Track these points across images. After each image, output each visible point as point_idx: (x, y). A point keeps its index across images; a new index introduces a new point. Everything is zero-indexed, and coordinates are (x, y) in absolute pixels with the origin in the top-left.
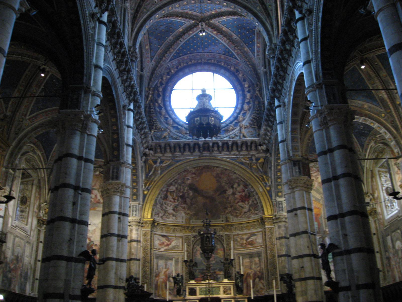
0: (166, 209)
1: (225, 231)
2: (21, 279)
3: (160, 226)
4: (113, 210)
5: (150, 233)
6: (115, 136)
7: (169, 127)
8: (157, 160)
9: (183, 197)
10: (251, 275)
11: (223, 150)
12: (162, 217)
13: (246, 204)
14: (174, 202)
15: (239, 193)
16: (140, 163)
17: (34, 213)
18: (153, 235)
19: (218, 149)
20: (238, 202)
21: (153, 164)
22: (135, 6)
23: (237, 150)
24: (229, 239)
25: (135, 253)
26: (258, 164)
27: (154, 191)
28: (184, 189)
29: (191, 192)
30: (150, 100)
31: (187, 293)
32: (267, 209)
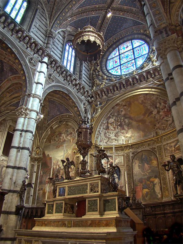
8: (97, 103)
11: (141, 81)
12: (106, 143)
14: (115, 130)
15: (163, 110)
19: (137, 82)
22: (51, 9)
28: (121, 120)
29: (126, 120)
30: (93, 70)
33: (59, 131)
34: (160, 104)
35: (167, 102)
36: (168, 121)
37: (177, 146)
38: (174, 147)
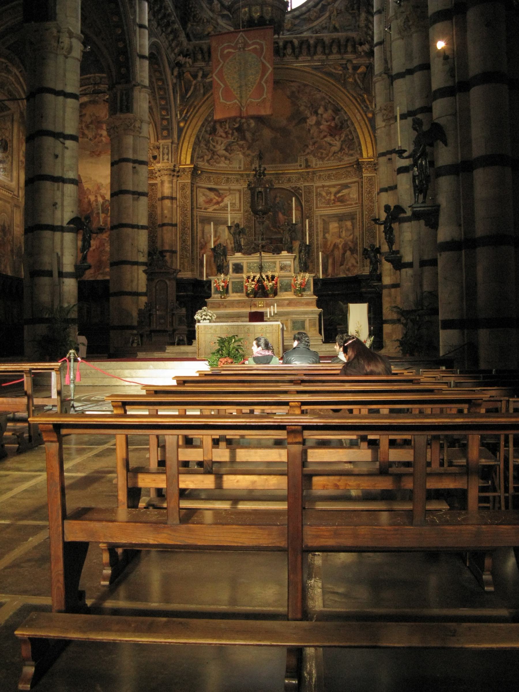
0: (215, 149)
1: (304, 182)
2: (13, 258)
3: (205, 175)
4: (125, 156)
5: (189, 186)
6: (121, 45)
7: (216, 16)
8: (198, 72)
9: (239, 130)
10: (340, 246)
11: (300, 52)
12: (208, 161)
13: (336, 140)
14: (227, 137)
15: (327, 122)
16: (171, 80)
17: (20, 163)
18: (195, 188)
20: (325, 137)
21: (192, 79)
23: (324, 53)
24: (310, 193)
25: (169, 216)
26: (356, 76)
27: (194, 121)
31: (231, 270)
32: (367, 147)
33: (94, 115)
34: (326, 110)
35: (339, 113)
36: (333, 146)
37: (340, 195)
38: (335, 196)
